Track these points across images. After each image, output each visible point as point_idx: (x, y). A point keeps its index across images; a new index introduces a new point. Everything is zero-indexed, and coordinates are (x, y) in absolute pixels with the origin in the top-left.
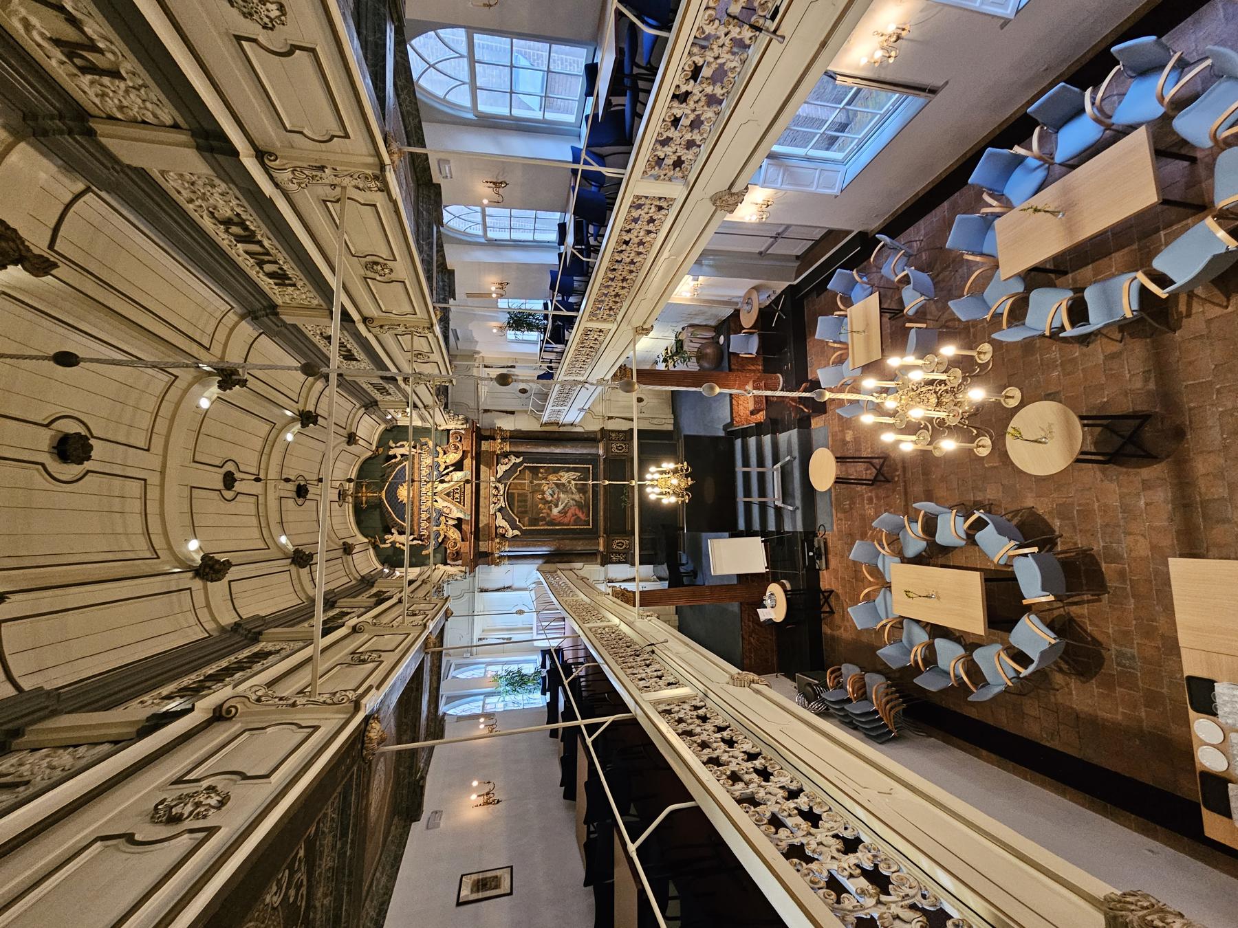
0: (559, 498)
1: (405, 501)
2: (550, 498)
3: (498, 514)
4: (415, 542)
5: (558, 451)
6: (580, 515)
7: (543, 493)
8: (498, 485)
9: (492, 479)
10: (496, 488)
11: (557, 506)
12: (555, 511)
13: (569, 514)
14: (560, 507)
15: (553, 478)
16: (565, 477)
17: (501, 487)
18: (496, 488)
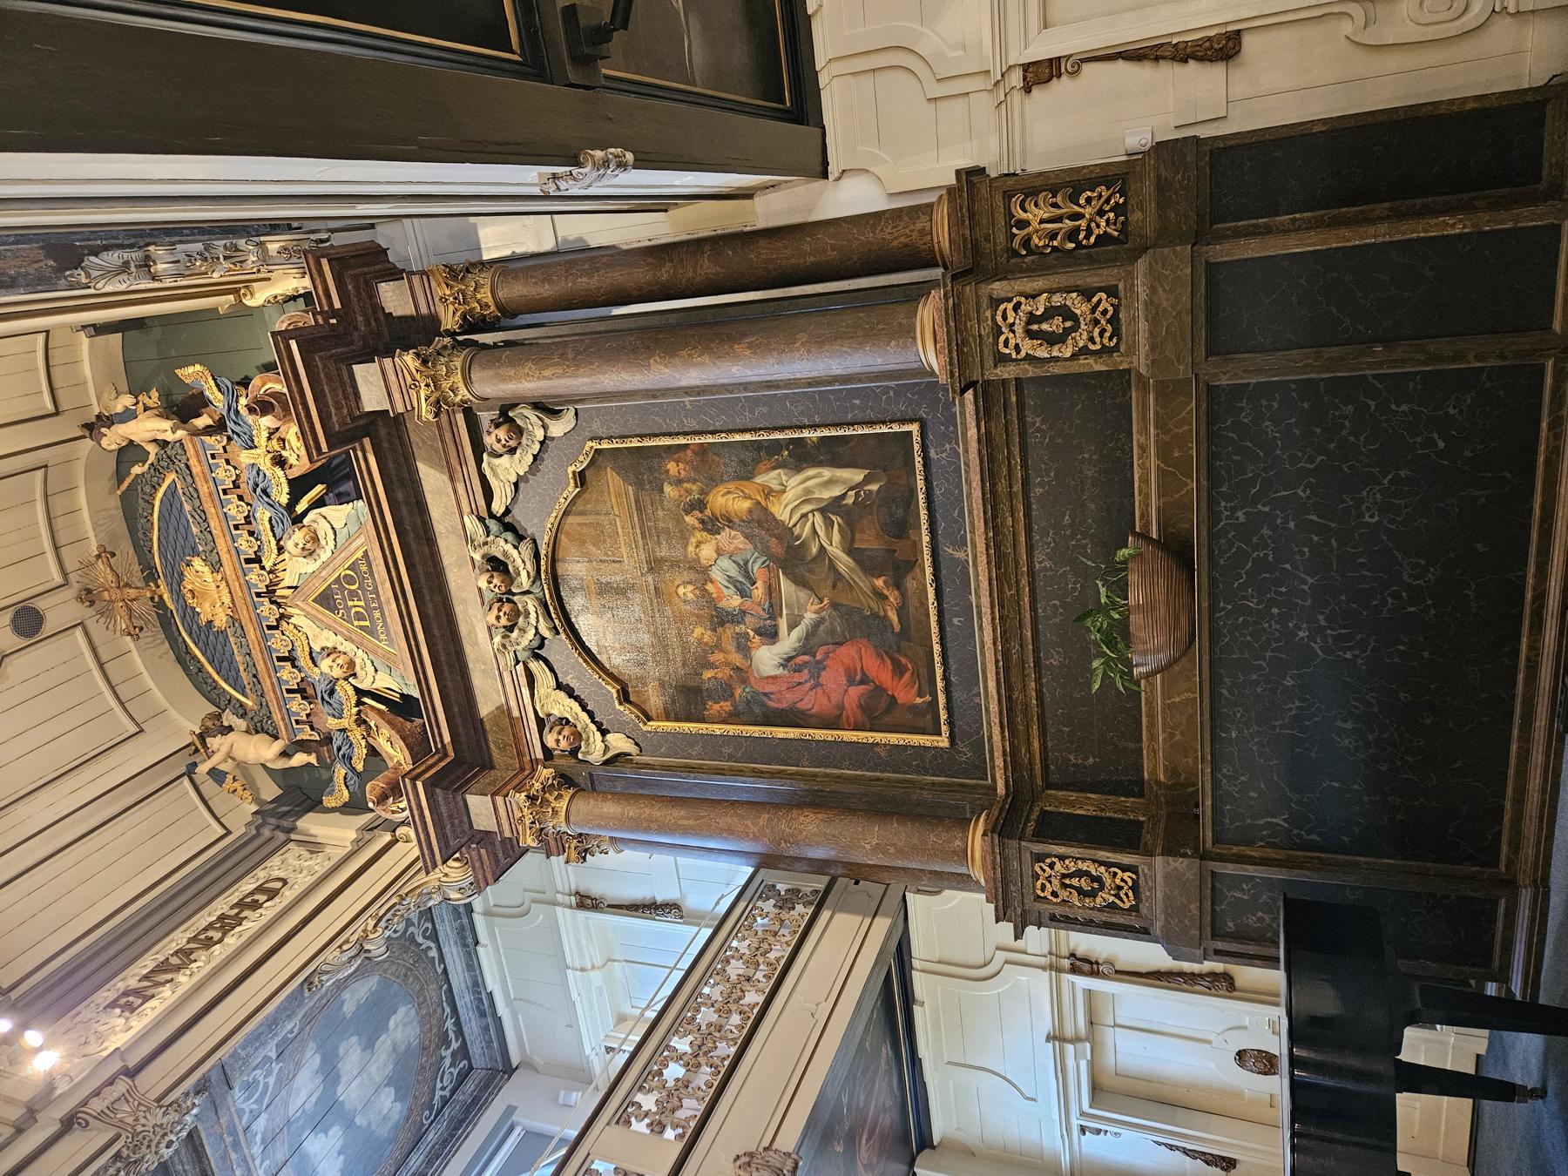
0: (774, 612)
1: (221, 621)
2: (734, 601)
3: (535, 666)
4: (300, 759)
5: (693, 376)
6: (881, 673)
7: (701, 573)
8: (503, 547)
9: (472, 524)
10: (497, 565)
11: (771, 635)
12: (767, 659)
13: (833, 678)
14: (789, 641)
15: (729, 500)
16: (796, 495)
17: (519, 559)
18: (497, 565)
